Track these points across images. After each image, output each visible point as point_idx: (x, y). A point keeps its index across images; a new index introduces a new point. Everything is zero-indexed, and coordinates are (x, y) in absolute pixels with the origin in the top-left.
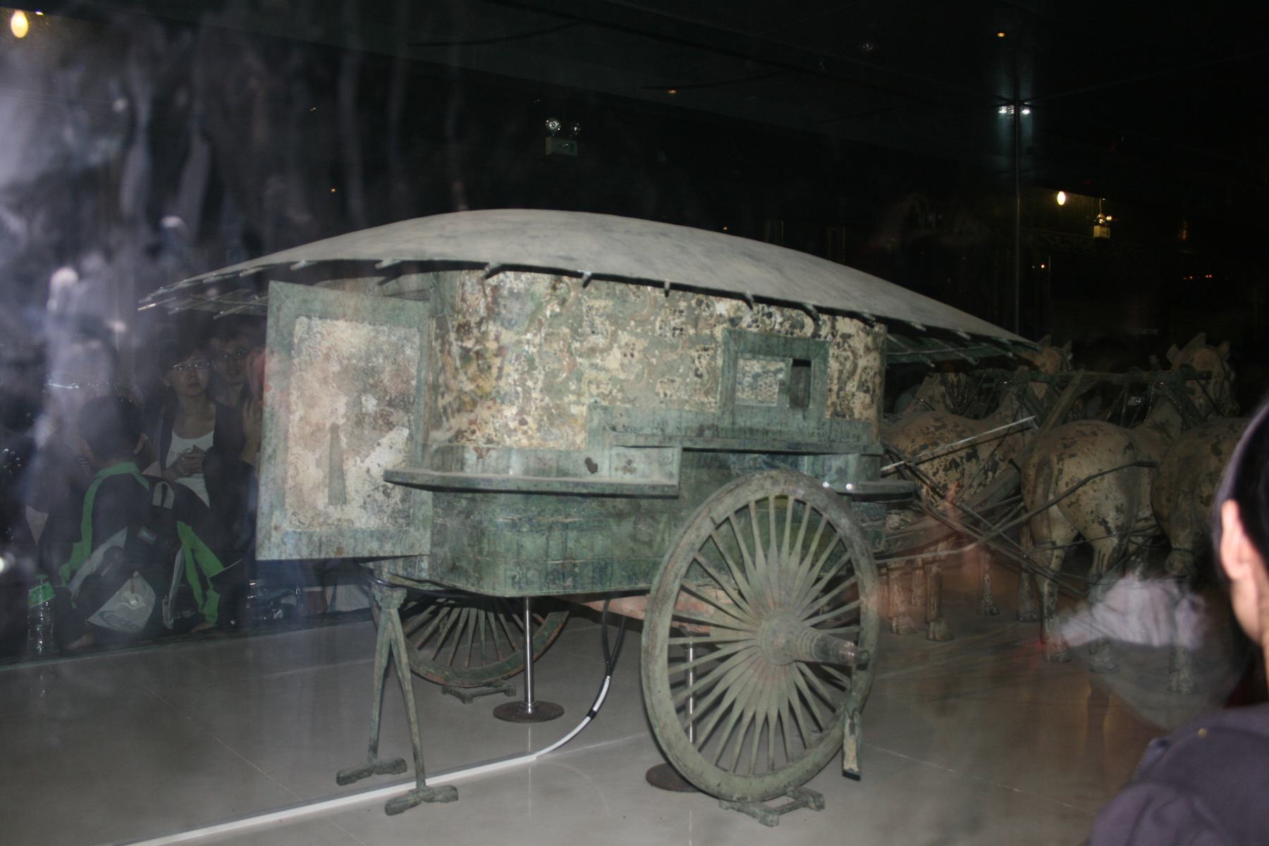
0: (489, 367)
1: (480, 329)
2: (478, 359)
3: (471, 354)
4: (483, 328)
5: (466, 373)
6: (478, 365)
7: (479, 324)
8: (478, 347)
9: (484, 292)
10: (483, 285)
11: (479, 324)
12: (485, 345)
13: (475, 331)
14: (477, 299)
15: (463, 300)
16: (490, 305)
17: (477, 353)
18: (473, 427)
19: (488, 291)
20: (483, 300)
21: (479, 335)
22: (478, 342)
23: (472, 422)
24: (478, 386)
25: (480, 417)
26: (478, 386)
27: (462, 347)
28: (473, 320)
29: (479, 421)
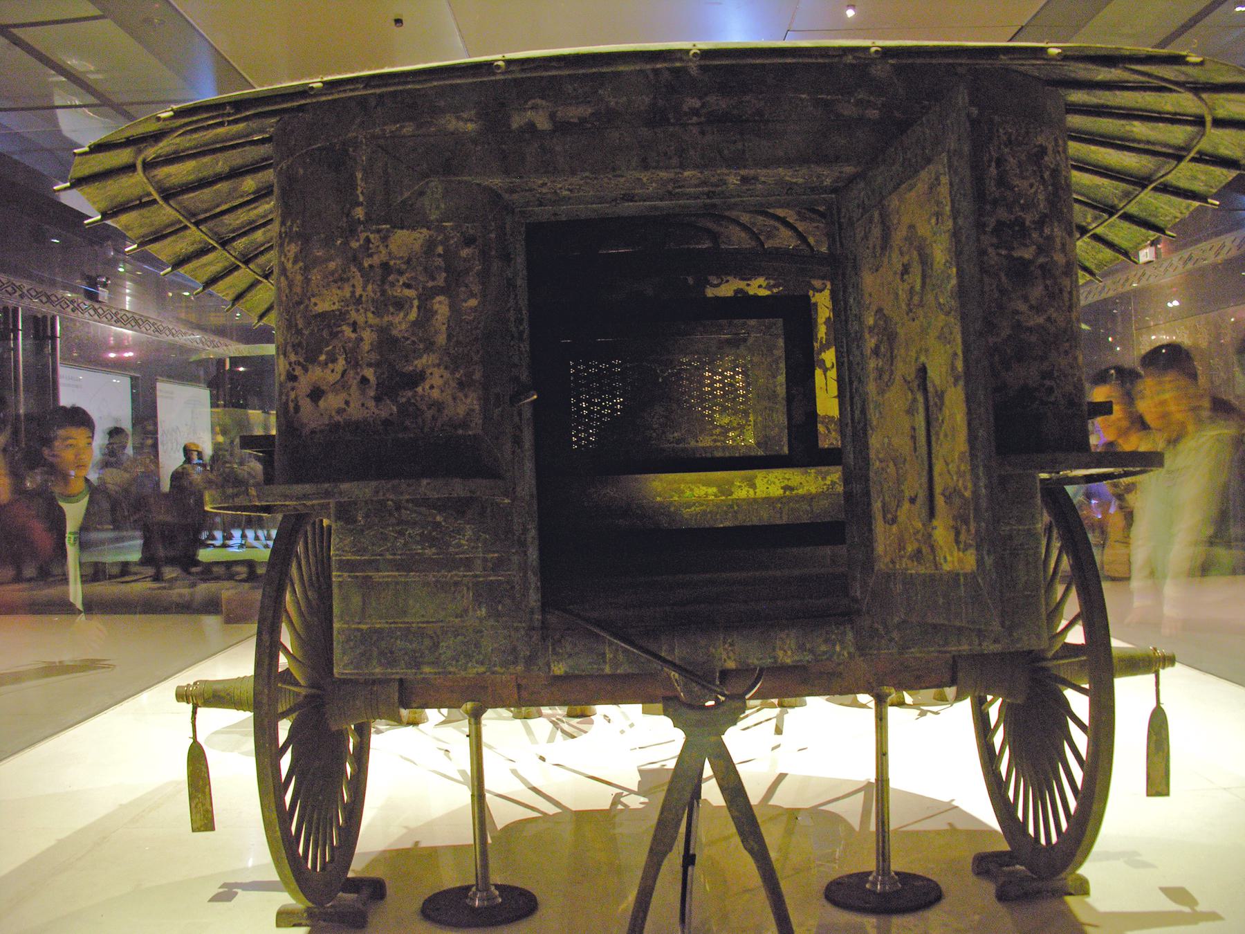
0: (1061, 291)
1: (1042, 231)
2: (1044, 278)
3: (1032, 268)
4: (1047, 231)
5: (1025, 299)
6: (1046, 287)
7: (1041, 223)
8: (1041, 260)
9: (1042, 177)
10: (1039, 167)
11: (1041, 223)
12: (1052, 258)
13: (1035, 235)
14: (1031, 186)
15: (1002, 181)
16: (1051, 197)
17: (1042, 267)
18: (1048, 383)
19: (1047, 175)
20: (1041, 187)
21: (1041, 240)
22: (1041, 250)
23: (1047, 375)
24: (1049, 319)
25: (1056, 368)
26: (1049, 319)
27: (1009, 257)
28: (1029, 218)
29: (1056, 374)
